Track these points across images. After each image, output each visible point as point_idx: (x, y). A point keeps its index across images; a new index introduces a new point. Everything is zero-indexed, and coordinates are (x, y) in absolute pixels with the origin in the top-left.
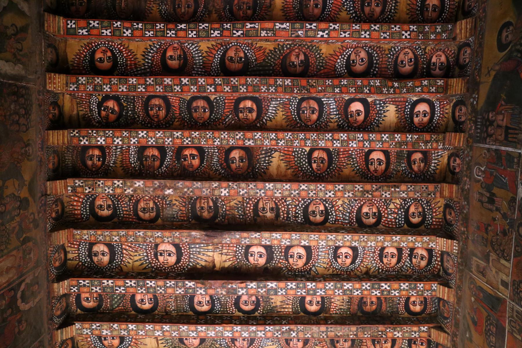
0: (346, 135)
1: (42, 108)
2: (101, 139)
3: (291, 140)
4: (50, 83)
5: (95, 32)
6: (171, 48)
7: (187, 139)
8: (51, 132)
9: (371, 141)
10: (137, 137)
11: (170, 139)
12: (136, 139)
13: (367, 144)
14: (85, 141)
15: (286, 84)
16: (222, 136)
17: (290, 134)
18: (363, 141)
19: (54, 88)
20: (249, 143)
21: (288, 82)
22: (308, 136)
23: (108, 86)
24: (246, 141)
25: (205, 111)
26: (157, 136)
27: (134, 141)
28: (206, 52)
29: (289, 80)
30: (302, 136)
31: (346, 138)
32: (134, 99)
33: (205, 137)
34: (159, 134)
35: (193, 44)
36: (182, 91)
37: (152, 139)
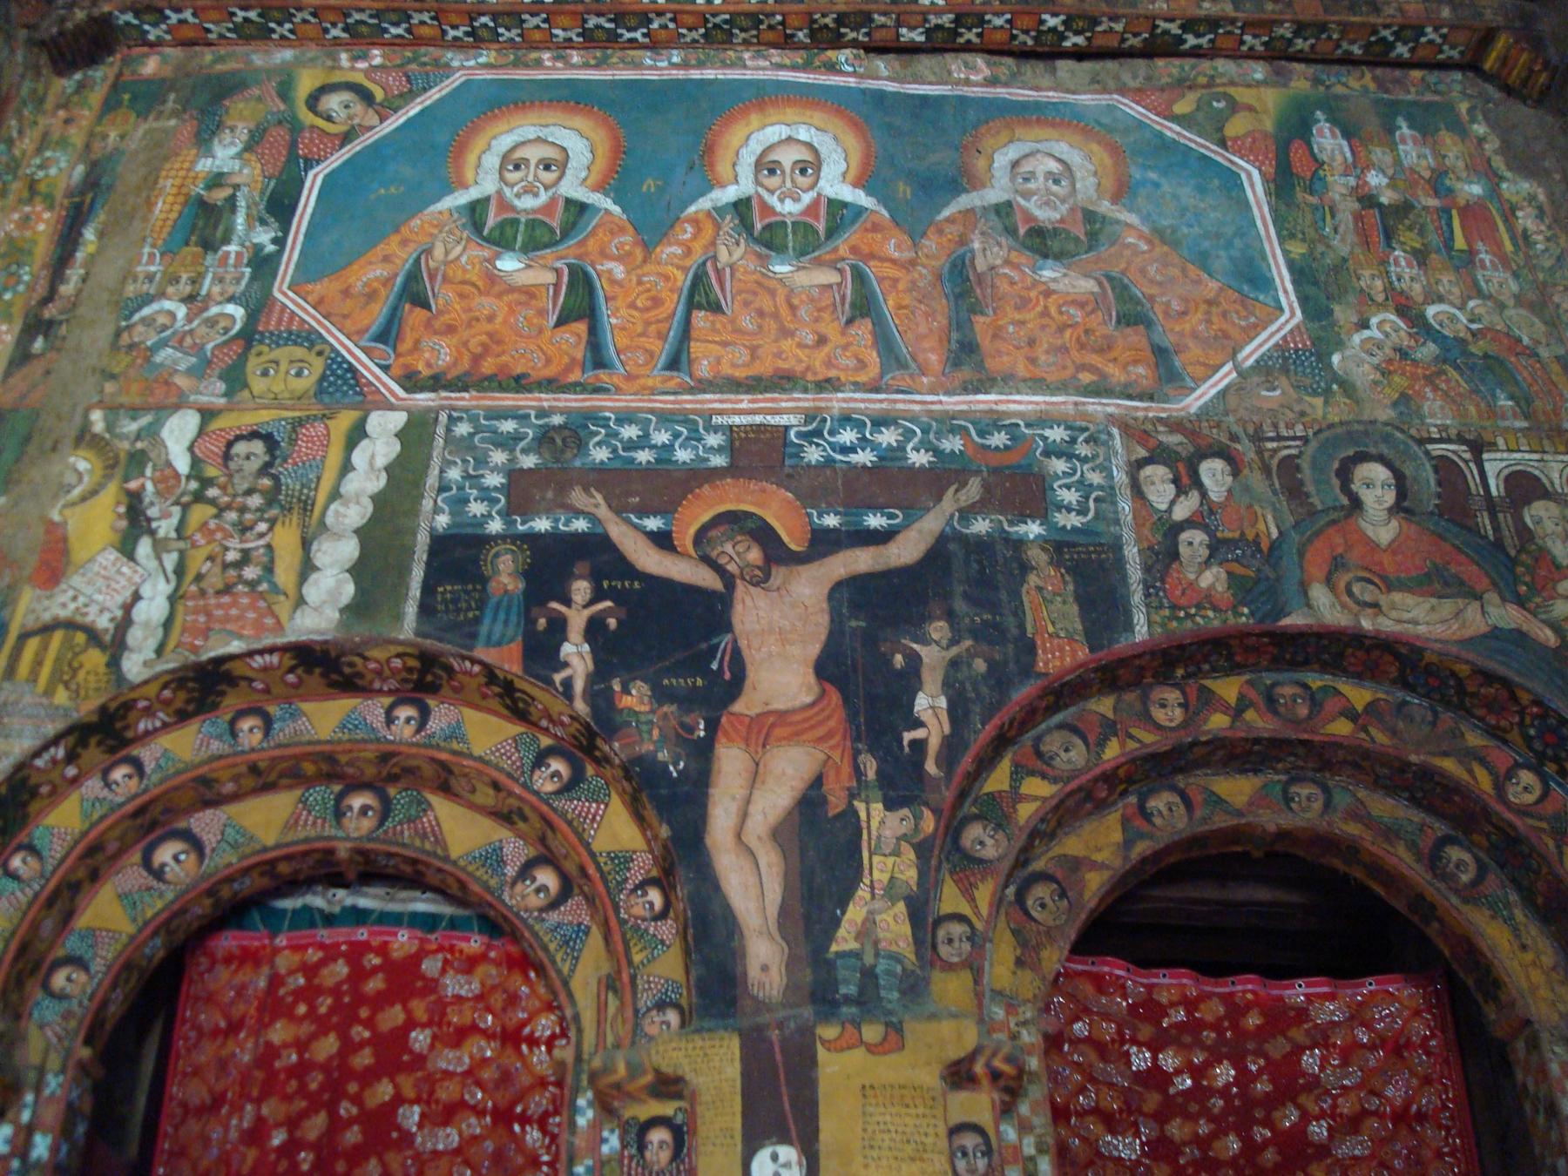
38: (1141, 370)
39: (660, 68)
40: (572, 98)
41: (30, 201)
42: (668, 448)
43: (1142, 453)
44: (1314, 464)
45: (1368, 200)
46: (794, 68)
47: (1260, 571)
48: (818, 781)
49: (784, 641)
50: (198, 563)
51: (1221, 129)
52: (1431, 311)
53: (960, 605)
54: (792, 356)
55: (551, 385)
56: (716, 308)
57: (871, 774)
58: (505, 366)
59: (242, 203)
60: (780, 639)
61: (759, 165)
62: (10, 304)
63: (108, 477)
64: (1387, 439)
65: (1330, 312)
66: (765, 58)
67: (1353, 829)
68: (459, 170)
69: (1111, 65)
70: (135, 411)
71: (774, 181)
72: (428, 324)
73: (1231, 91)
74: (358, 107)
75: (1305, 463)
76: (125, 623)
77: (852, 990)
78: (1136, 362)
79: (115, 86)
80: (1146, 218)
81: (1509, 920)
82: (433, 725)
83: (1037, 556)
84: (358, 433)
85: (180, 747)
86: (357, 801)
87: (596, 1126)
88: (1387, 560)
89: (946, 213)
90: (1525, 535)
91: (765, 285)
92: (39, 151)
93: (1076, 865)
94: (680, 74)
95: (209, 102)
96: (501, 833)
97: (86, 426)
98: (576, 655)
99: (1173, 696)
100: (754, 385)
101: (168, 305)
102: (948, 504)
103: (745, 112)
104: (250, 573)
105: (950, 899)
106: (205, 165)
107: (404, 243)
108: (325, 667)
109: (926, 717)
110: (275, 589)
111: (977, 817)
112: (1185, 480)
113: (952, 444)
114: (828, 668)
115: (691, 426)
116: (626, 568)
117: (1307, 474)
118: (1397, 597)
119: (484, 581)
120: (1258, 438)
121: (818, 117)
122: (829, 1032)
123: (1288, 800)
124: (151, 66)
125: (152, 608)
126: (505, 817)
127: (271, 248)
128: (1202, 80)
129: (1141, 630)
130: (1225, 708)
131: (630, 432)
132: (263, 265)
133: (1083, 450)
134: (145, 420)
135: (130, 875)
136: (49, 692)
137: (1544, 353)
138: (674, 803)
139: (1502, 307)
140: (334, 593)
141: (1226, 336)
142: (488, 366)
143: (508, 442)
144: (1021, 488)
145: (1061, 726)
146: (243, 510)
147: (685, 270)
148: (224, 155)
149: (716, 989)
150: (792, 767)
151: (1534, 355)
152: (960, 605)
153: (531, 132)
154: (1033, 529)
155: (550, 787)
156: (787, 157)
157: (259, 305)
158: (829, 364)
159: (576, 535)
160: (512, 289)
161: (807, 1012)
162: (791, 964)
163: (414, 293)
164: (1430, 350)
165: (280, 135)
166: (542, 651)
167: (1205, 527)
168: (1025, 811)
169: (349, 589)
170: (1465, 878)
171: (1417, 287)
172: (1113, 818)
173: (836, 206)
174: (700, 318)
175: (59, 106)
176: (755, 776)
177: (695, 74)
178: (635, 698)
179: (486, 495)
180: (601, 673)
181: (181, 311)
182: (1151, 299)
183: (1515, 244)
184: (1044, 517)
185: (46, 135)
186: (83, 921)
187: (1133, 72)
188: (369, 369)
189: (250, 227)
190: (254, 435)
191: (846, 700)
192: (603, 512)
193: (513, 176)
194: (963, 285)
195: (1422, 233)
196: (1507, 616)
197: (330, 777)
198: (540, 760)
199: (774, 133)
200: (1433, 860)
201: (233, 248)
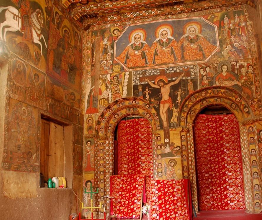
38: (201, 57)
39: (149, 21)
40: (140, 28)
41: (87, 50)
42: (154, 73)
43: (200, 68)
44: (219, 67)
45: (229, 28)
46: (164, 19)
48: (169, 107)
49: (166, 93)
50: (113, 91)
51: (213, 21)
52: (235, 44)
53: (182, 87)
54: (165, 60)
55: (142, 67)
56: (157, 55)
57: (174, 106)
58: (137, 65)
59: (109, 47)
60: (165, 93)
64: (227, 62)
65: (223, 46)
66: (161, 18)
67: (223, 103)
68: (130, 40)
69: (201, 12)
70: (104, 75)
71: (163, 36)
72: (130, 61)
74: (118, 32)
75: (217, 67)
76: (108, 98)
77: (172, 126)
78: (201, 56)
79: (92, 31)
80: (203, 36)
81: (238, 112)
82: (136, 103)
83: (189, 81)
84: (125, 75)
85: (115, 107)
86: (131, 109)
87: (154, 136)
88: (224, 77)
89: (181, 38)
90: (240, 72)
91: (162, 51)
92: (87, 42)
93: (196, 109)
94: (152, 22)
96: (144, 111)
97: (100, 77)
98: (147, 96)
99: (204, 93)
100: (162, 64)
101: (104, 61)
102: (181, 76)
103: (159, 27)
104: (118, 91)
105: (182, 115)
106: (104, 43)
107: (126, 51)
108: (125, 99)
110: (120, 93)
111: (185, 107)
112: (205, 70)
113: (181, 69)
114: (170, 95)
116: (151, 87)
117: (217, 68)
118: (225, 82)
119: (138, 90)
120: (213, 64)
121: (167, 27)
122: (170, 129)
123: (217, 101)
124: (95, 29)
125: (110, 96)
126: (144, 110)
127: (113, 53)
128: (212, 13)
131: (150, 71)
132: (112, 55)
133: (194, 68)
134: (105, 75)
135: (113, 118)
137: (247, 48)
138: (158, 110)
139: (243, 42)
141: (211, 51)
142: (136, 65)
143: (139, 74)
144: (188, 73)
147: (154, 50)
148: (106, 41)
149: (161, 126)
150: (167, 105)
152: (182, 87)
153: (136, 33)
154: (189, 78)
155: (147, 107)
156: (164, 33)
157: (113, 60)
158: (169, 61)
160: (137, 56)
161: (169, 128)
163: (128, 58)
164: (234, 49)
165: (111, 37)
166: (144, 96)
167: (206, 76)
168: (189, 106)
169: (127, 92)
170: (234, 107)
171: (234, 41)
172: (200, 104)
173: (169, 39)
174: (156, 56)
175: (87, 36)
176: (164, 107)
177: (153, 22)
178: (153, 100)
180: (150, 98)
181: (106, 62)
182: (203, 47)
183: (247, 32)
184: (190, 76)
185: (87, 40)
186: (110, 123)
188: (125, 67)
190: (115, 76)
191: (172, 99)
192: (148, 81)
193: (135, 40)
194: (183, 48)
195: (236, 33)
196: (236, 82)
197: (129, 107)
198: (146, 105)
199: (162, 30)
200: (231, 106)
201: (109, 53)
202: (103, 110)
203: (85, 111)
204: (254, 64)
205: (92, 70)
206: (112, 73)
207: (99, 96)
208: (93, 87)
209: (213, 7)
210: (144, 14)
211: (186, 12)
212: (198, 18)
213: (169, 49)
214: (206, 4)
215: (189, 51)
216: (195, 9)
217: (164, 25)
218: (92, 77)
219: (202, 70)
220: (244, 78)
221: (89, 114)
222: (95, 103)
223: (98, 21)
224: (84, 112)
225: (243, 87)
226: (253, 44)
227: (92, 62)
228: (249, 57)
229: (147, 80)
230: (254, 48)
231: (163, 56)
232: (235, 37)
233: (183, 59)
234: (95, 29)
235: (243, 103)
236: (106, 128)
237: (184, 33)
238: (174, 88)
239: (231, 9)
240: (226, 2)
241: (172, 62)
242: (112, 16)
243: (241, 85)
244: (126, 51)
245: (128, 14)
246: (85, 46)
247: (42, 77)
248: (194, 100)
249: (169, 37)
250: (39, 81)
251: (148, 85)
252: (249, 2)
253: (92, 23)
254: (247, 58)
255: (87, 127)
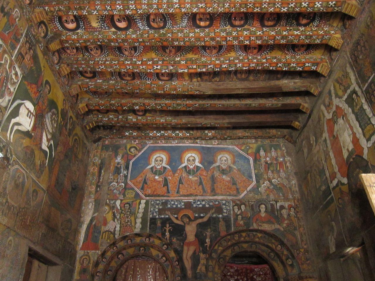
0: (127, 13)
1: (351, 33)
2: (318, 6)
3: (169, 8)
4: (340, 44)
5: (300, 65)
6: (254, 53)
7: (250, 7)
8: (353, 15)
9: (106, 9)
10: (289, 8)
11: (263, 6)
12: (290, 6)
13: (108, 8)
14: (331, 4)
15: (177, 43)
16: (223, 9)
17: (171, 12)
18: (112, 10)
19: (338, 40)
20: (202, 5)
21: (176, 43)
22: (157, 11)
23: (301, 38)
24: (204, 6)
25: (235, 18)
26: (273, 9)
27: (292, 5)
28: (231, 51)
29: (175, 44)
30: (161, 11)
31: (126, 11)
32: (286, 26)
33: (236, 8)
34: (271, 10)
35: (240, 55)
36: (250, 37)
37: (278, 7)
40: (163, 149)
41: (94, 166)
42: (177, 205)
43: (234, 204)
45: (266, 162)
46: (192, 143)
47: (248, 221)
48: (195, 251)
52: (273, 180)
53: (212, 227)
54: (192, 191)
55: (163, 196)
56: (183, 184)
60: (191, 230)
61: (188, 160)
62: (94, 182)
63: (110, 210)
64: (265, 201)
65: (259, 182)
66: (188, 141)
67: (259, 251)
68: (149, 162)
69: (234, 140)
70: (112, 200)
71: (189, 163)
72: (147, 187)
73: (250, 145)
74: (136, 151)
75: (254, 205)
76: (115, 230)
81: (277, 263)
82: (151, 241)
83: (221, 220)
84: (140, 203)
85: (122, 244)
86: (142, 249)
89: (211, 167)
90: (281, 214)
91: (189, 180)
92: (94, 157)
93: (225, 256)
94: (177, 145)
95: (116, 149)
96: (159, 253)
98: (167, 234)
99: (237, 236)
100: (187, 196)
101: (114, 183)
103: (185, 152)
104: (129, 223)
105: (210, 263)
106: (116, 161)
108: (138, 235)
109: (207, 242)
113: (211, 204)
114: (196, 236)
115: (180, 201)
116: (173, 222)
117: (254, 207)
118: (264, 224)
119: (156, 224)
121: (195, 152)
123: (251, 247)
125: (118, 228)
129: (233, 230)
130: (243, 237)
131: (173, 203)
132: (126, 177)
133: (227, 204)
134: (114, 201)
136: (107, 240)
137: (287, 186)
138: (179, 253)
139: (282, 179)
140: (139, 226)
142: (155, 193)
143: (158, 204)
144: (219, 210)
145: (224, 240)
146: (127, 214)
148: (119, 159)
150: (192, 249)
151: (286, 186)
152: (212, 227)
153: (158, 155)
154: (221, 216)
155: (165, 249)
156: (191, 159)
157: (126, 184)
158: (196, 192)
159: (167, 218)
162: (192, 274)
163: (145, 182)
165: (126, 156)
166: (164, 234)
168: (219, 251)
170: (272, 257)
173: (197, 167)
175: (96, 149)
176: (188, 250)
177: (179, 145)
178: (174, 240)
179: (156, 212)
180: (170, 237)
185: (94, 154)
186: (111, 265)
187: (237, 142)
189: (123, 171)
190: (127, 203)
191: (199, 241)
192: (170, 214)
194: (213, 179)
196: (277, 226)
198: (163, 245)
200: (269, 255)
201: (122, 174)
202: (105, 247)
203: (80, 246)
204: (296, 205)
205: (96, 191)
206: (123, 198)
207: (103, 227)
208: (96, 214)
209: (248, 138)
210: (170, 135)
211: (217, 139)
212: (230, 146)
213: (196, 178)
214: (241, 133)
215: (220, 183)
216: (228, 137)
217: (191, 150)
218: (95, 201)
219: (236, 207)
220: (286, 222)
221: (86, 251)
222: (96, 236)
223: (113, 134)
224: (78, 246)
225: (285, 233)
226: (293, 182)
227: (99, 182)
228: (290, 197)
229: (169, 213)
230: (295, 187)
231: (189, 186)
232: (273, 173)
233: (214, 192)
234: (107, 142)
235: (285, 252)
236: (106, 271)
237: (214, 162)
238: (202, 226)
239: (267, 142)
240: (263, 134)
241: (200, 194)
242: (131, 132)
243: (282, 229)
244: (143, 174)
245: (151, 132)
246: (91, 161)
247: (41, 194)
248: (225, 244)
249: (197, 164)
250: (37, 200)
251: (169, 219)
252: (287, 137)
253: (105, 135)
254: (288, 199)
255: (79, 269)
